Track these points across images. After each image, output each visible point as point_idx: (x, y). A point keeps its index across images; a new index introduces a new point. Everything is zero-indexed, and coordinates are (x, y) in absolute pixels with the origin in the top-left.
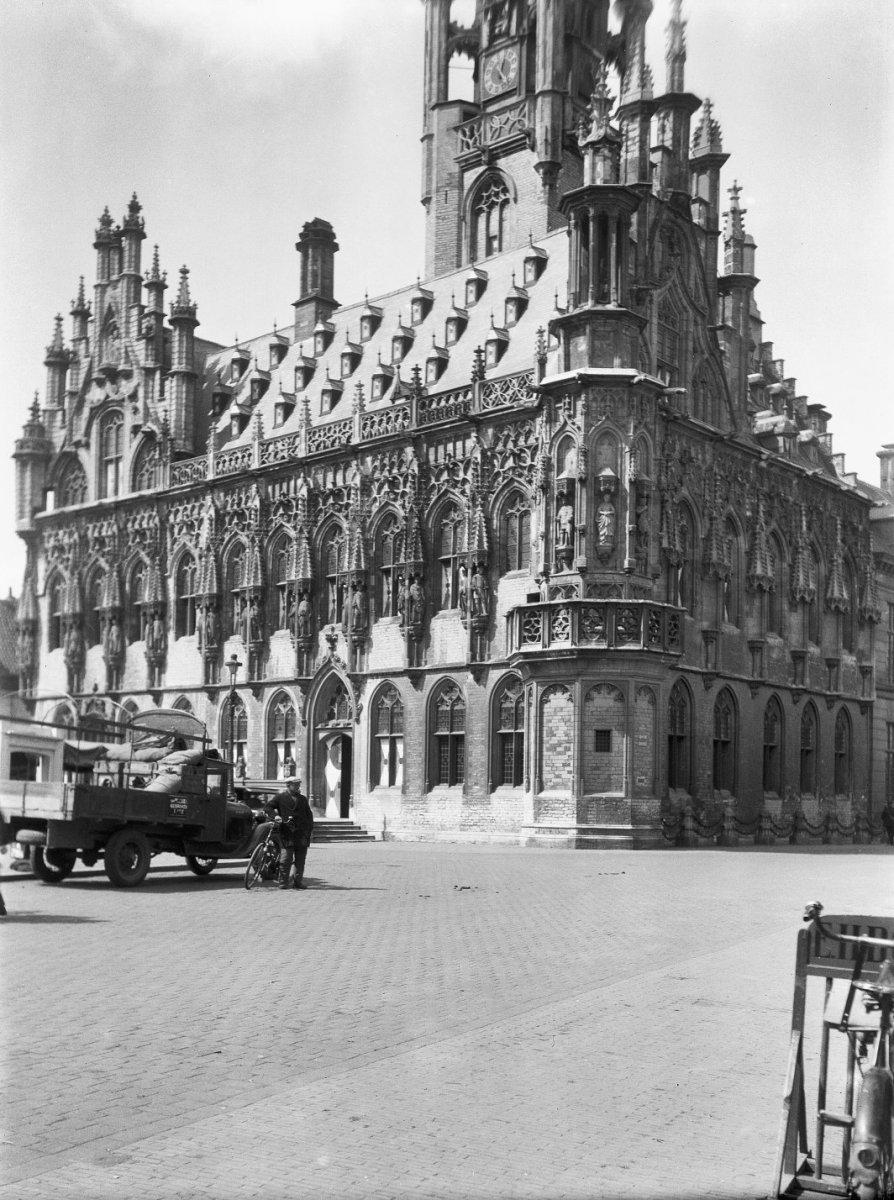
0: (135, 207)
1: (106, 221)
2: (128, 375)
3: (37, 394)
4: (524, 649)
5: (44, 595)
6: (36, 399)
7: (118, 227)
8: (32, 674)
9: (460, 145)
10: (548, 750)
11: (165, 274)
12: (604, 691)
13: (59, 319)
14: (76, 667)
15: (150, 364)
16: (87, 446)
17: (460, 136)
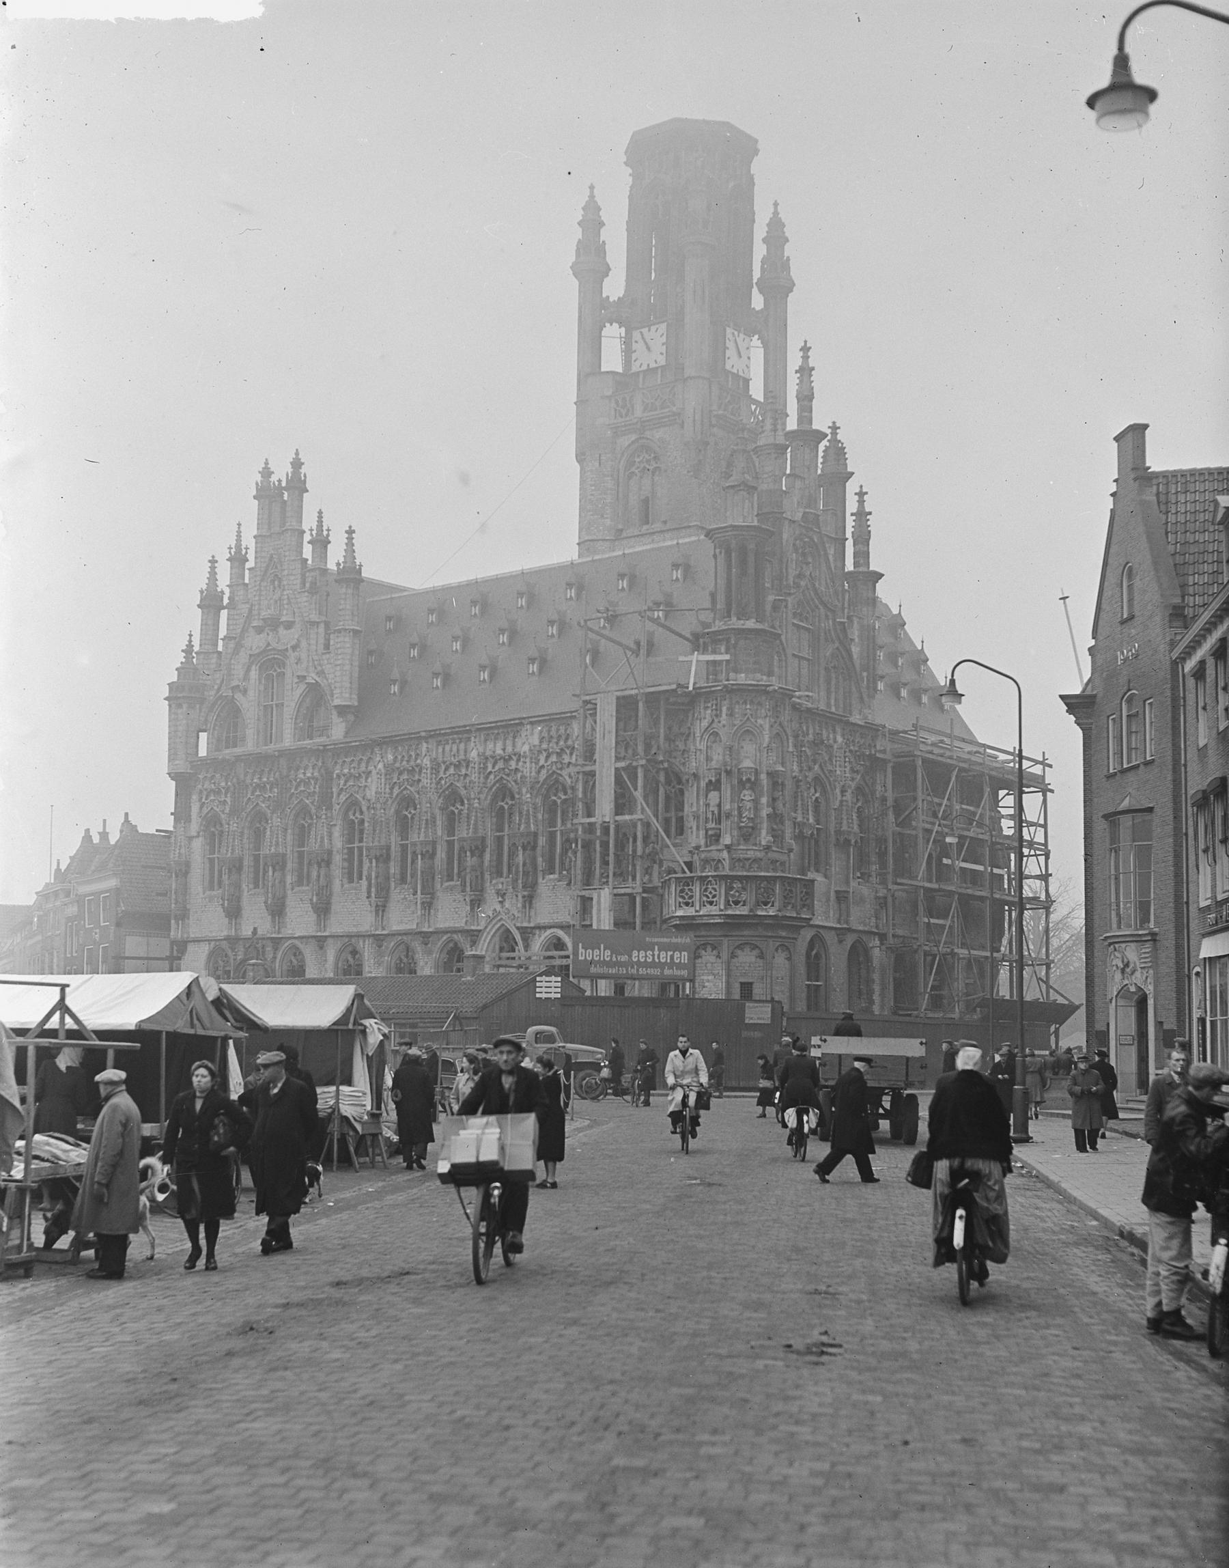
0: (297, 464)
1: (266, 472)
2: (289, 625)
3: (191, 635)
5: (198, 836)
6: (190, 641)
9: (613, 412)
11: (328, 530)
12: (747, 949)
13: (213, 562)
15: (314, 617)
16: (245, 692)
17: (613, 405)
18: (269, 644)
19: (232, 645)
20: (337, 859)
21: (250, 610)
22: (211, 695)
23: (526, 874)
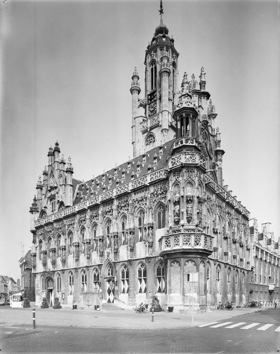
3: (35, 196)
6: (35, 197)
8: (35, 267)
18: (52, 194)
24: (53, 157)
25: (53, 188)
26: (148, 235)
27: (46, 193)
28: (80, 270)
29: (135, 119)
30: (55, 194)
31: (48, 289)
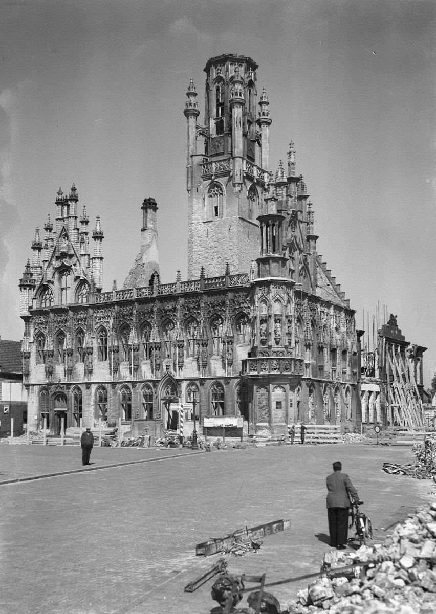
1: (60, 193)
2: (71, 256)
4: (251, 374)
7: (66, 196)
10: (259, 408)
12: (279, 388)
14: (50, 372)
16: (53, 283)
18: (63, 263)
19: (46, 264)
20: (95, 351)
21: (55, 249)
22: (38, 284)
23: (180, 357)
24: (66, 208)
25: (64, 255)
26: (228, 351)
27: (51, 259)
28: (119, 386)
29: (192, 156)
30: (71, 266)
31: (55, 411)
